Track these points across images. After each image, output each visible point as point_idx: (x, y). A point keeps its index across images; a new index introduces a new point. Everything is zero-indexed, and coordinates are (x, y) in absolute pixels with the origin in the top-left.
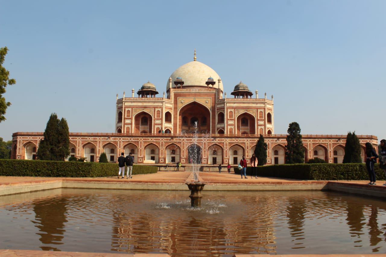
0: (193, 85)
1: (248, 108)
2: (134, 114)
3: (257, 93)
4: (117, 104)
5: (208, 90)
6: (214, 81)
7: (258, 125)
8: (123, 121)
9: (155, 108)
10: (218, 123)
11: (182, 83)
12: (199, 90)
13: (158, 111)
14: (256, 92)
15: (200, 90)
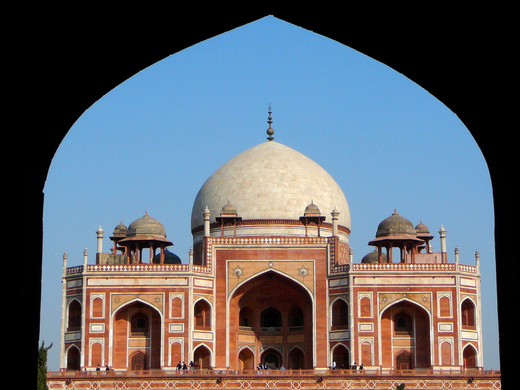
0: (266, 218)
1: (412, 289)
2: (114, 308)
3: (443, 235)
4: (64, 281)
5: (307, 239)
6: (321, 215)
7: (437, 334)
8: (83, 327)
9: (167, 291)
10: (333, 328)
11: (241, 218)
12: (283, 240)
13: (177, 300)
14: (440, 233)
15: (284, 242)
